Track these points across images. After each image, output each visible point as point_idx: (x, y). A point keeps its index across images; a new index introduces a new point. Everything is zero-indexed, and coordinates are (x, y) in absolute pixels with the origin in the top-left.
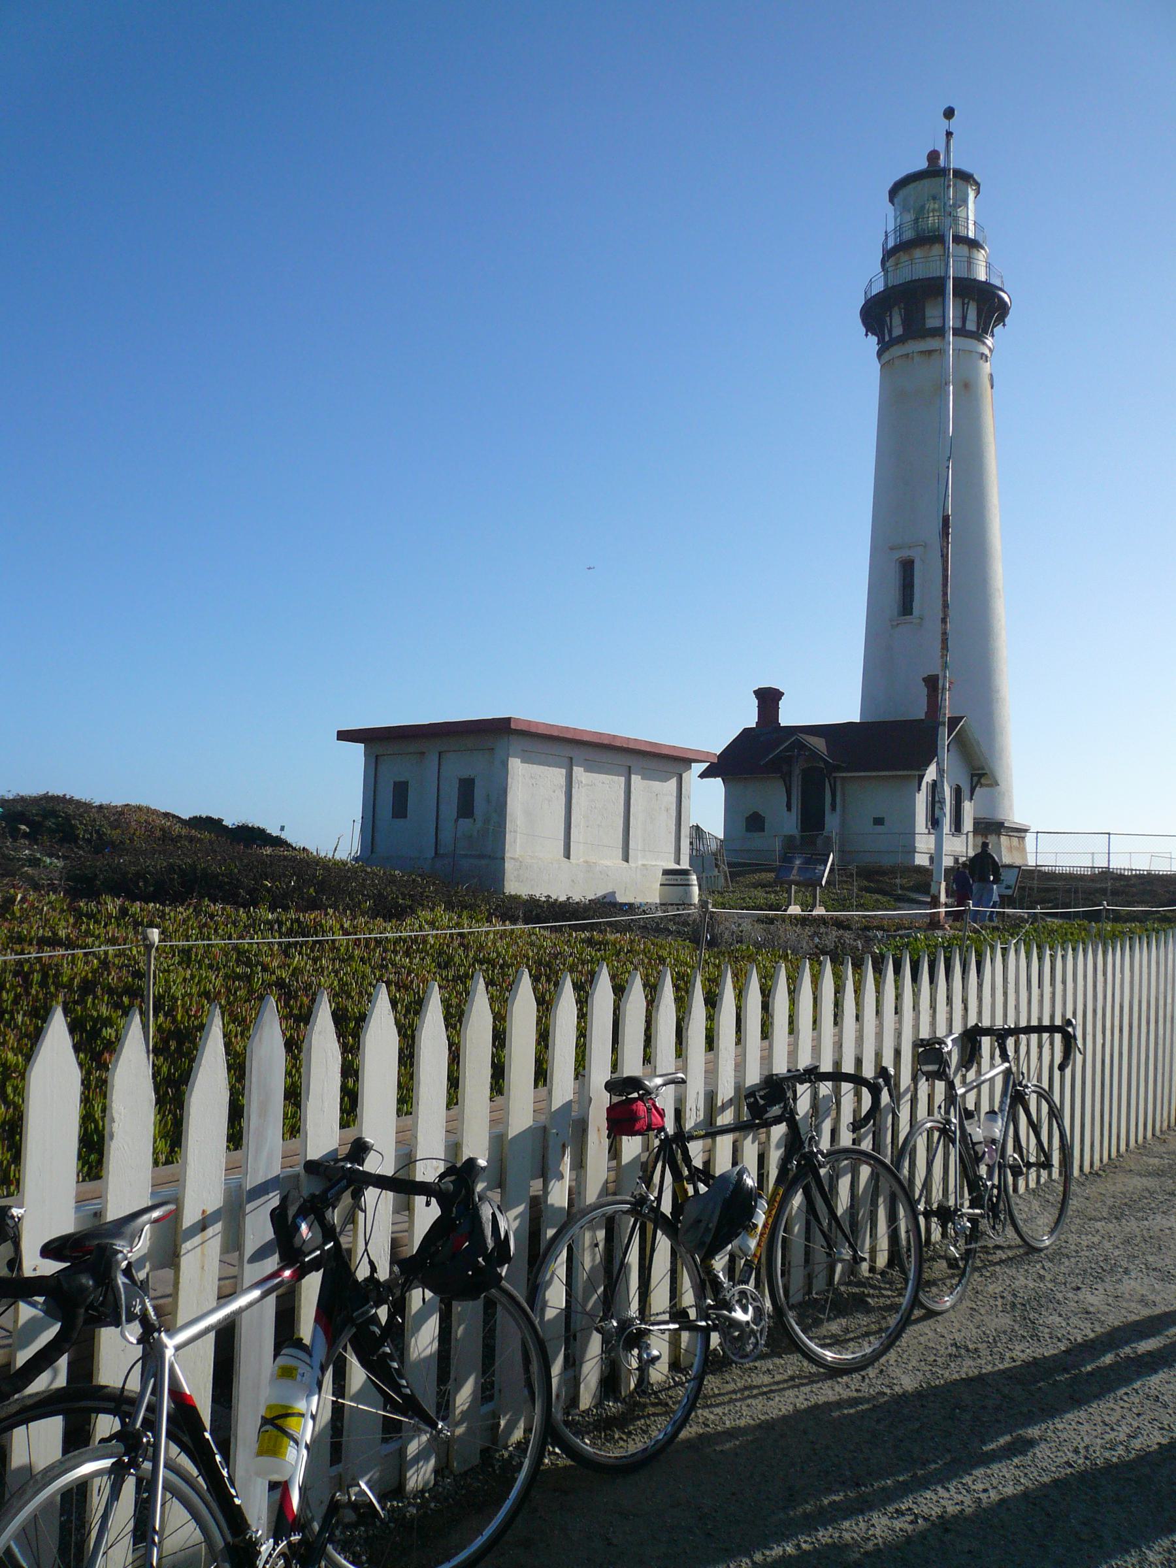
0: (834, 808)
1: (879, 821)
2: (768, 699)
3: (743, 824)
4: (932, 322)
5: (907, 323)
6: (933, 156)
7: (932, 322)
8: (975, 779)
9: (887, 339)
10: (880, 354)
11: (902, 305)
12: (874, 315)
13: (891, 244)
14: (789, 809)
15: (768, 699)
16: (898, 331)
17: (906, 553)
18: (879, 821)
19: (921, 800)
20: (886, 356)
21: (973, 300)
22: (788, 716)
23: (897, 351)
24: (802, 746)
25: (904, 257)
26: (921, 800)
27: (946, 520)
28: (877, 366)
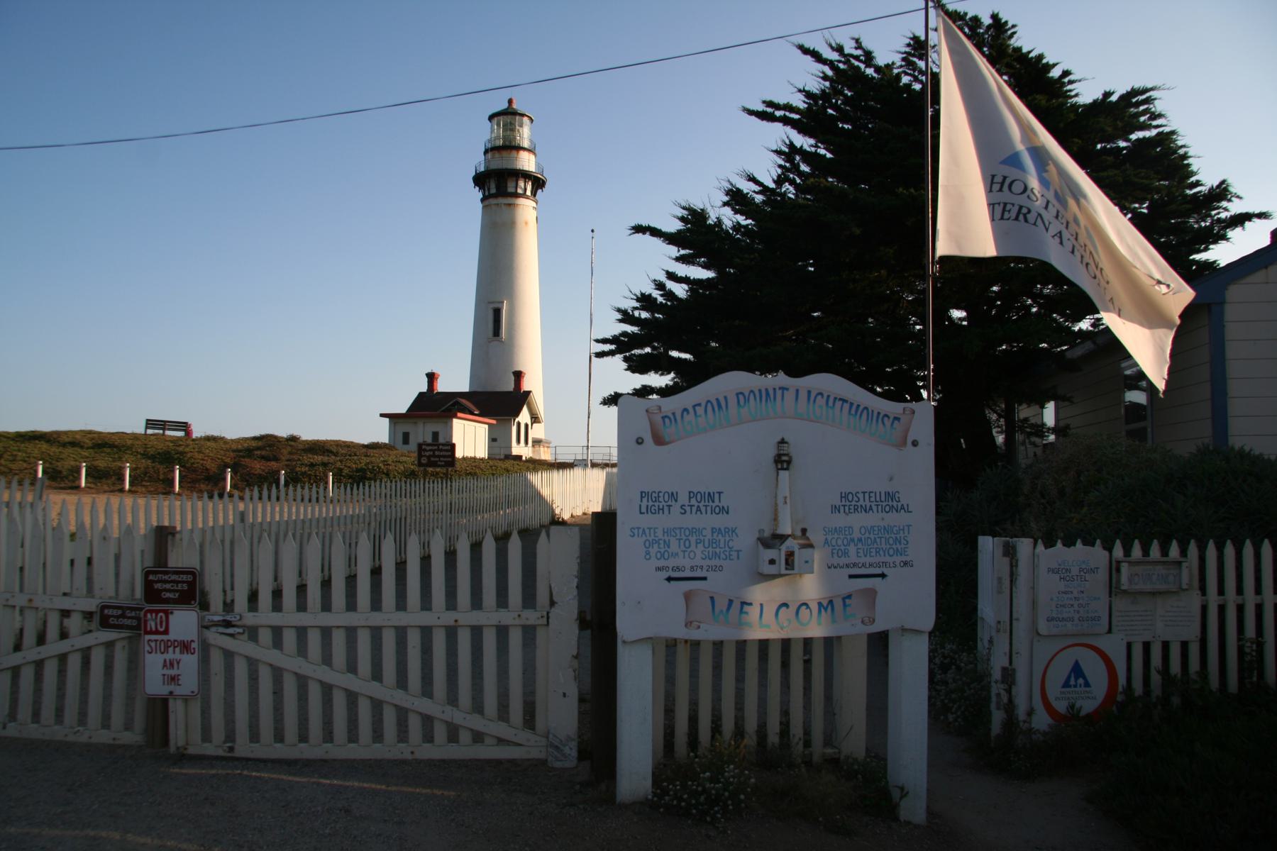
2: (431, 377)
4: (511, 190)
5: (498, 188)
7: (511, 190)
10: (482, 200)
12: (480, 180)
15: (431, 377)
16: (493, 191)
17: (496, 306)
19: (514, 429)
20: (487, 202)
22: (442, 386)
24: (457, 403)
25: (497, 155)
26: (514, 429)
28: (480, 205)
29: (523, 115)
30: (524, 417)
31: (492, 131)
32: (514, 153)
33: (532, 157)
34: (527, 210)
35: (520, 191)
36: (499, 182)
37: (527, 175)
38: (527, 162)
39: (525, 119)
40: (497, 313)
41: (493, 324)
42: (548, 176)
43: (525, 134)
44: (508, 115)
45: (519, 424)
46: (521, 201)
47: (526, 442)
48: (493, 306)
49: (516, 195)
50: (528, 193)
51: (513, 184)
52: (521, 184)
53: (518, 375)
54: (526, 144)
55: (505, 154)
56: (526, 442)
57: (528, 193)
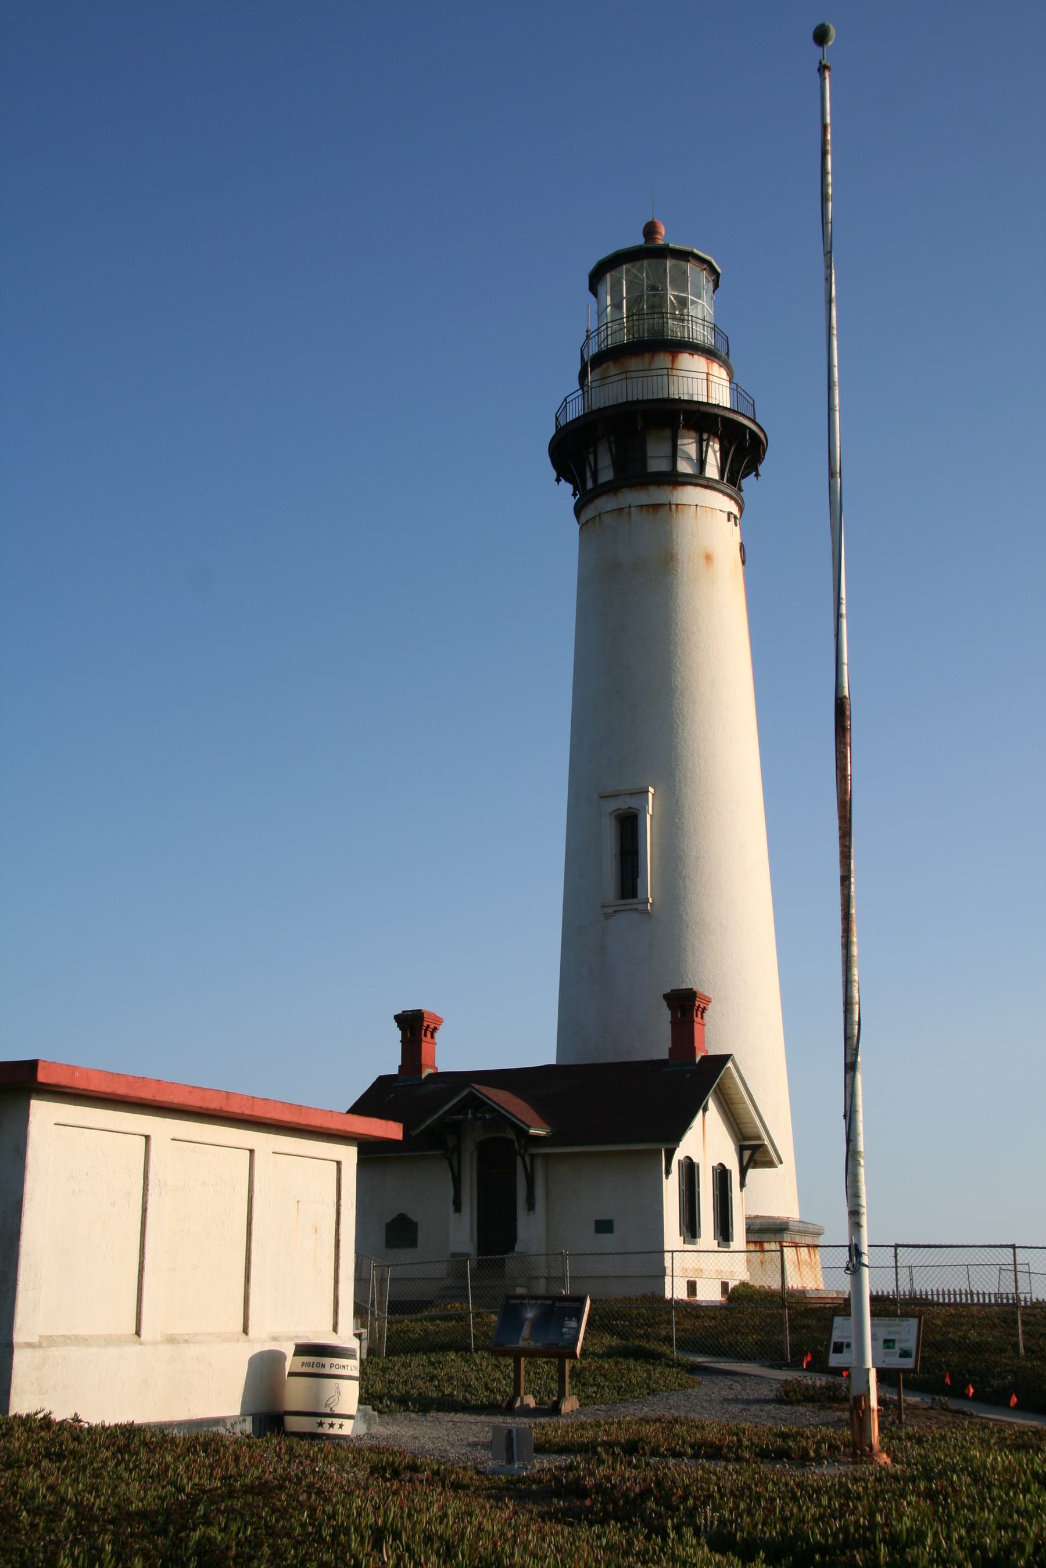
0: (531, 1205)
1: (604, 1226)
3: (379, 1235)
4: (657, 465)
5: (618, 465)
6: (650, 230)
7: (657, 465)
8: (747, 1154)
9: (590, 485)
11: (613, 439)
13: (593, 349)
14: (457, 1206)
16: (607, 475)
17: (625, 804)
18: (604, 1226)
19: (671, 1188)
20: (589, 512)
21: (716, 435)
22: (450, 1054)
23: (605, 503)
24: (477, 1103)
25: (612, 369)
26: (671, 1188)
27: (841, 707)
28: (577, 527)
29: (685, 256)
30: (707, 1141)
31: (601, 313)
32: (663, 360)
33: (719, 373)
34: (710, 525)
35: (684, 467)
36: (620, 449)
37: (702, 419)
38: (706, 383)
39: (704, 278)
40: (629, 825)
41: (623, 864)
42: (769, 421)
43: (700, 314)
44: (647, 258)
45: (690, 1169)
46: (691, 495)
47: (724, 1232)
48: (613, 805)
49: (677, 480)
50: (712, 471)
51: (666, 449)
52: (689, 446)
53: (685, 1006)
54: (701, 334)
55: (633, 364)
56: (724, 1232)
57: (712, 471)
